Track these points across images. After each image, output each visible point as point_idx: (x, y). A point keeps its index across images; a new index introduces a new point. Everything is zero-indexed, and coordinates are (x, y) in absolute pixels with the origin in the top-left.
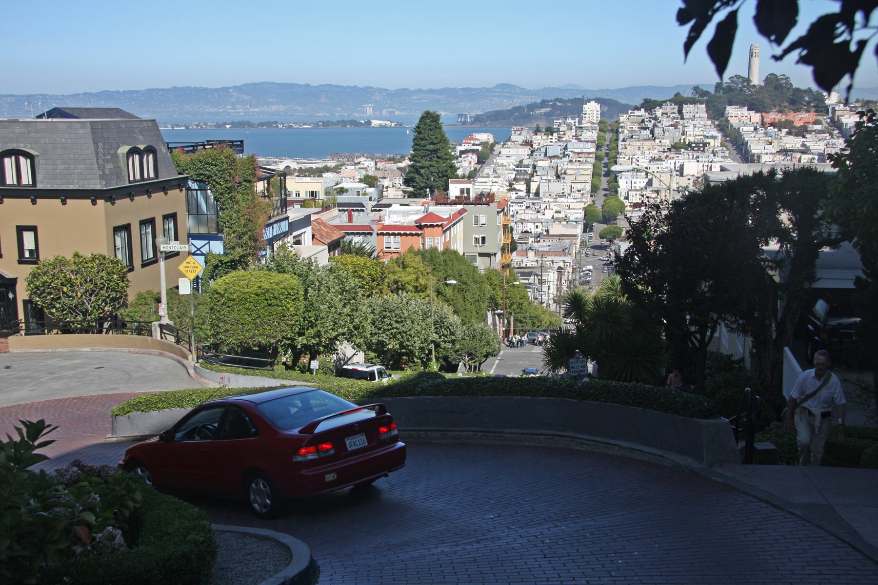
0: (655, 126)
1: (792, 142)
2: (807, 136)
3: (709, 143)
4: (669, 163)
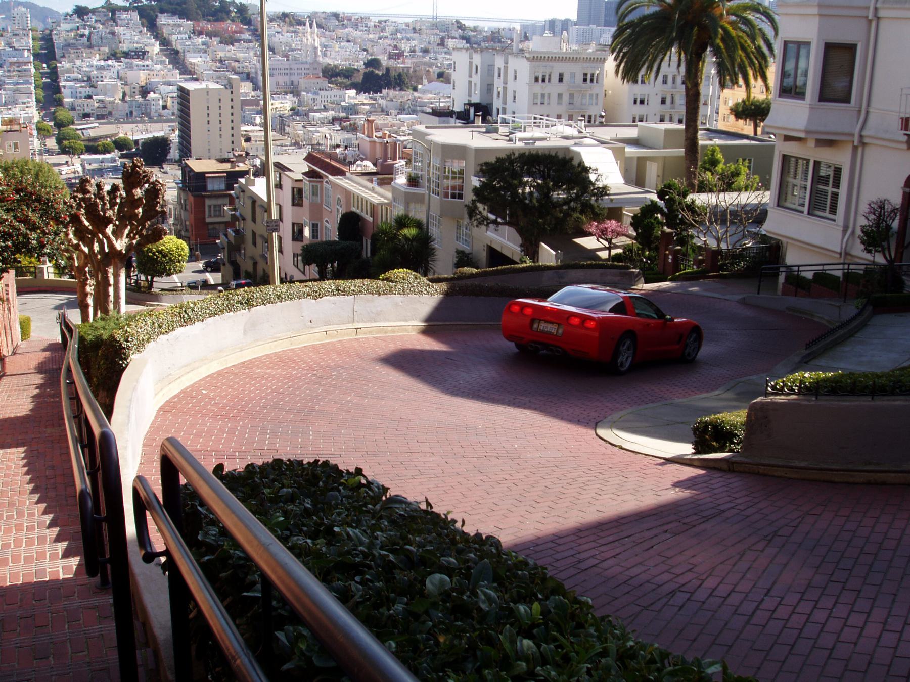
0: (90, 33)
1: (224, 52)
2: (235, 44)
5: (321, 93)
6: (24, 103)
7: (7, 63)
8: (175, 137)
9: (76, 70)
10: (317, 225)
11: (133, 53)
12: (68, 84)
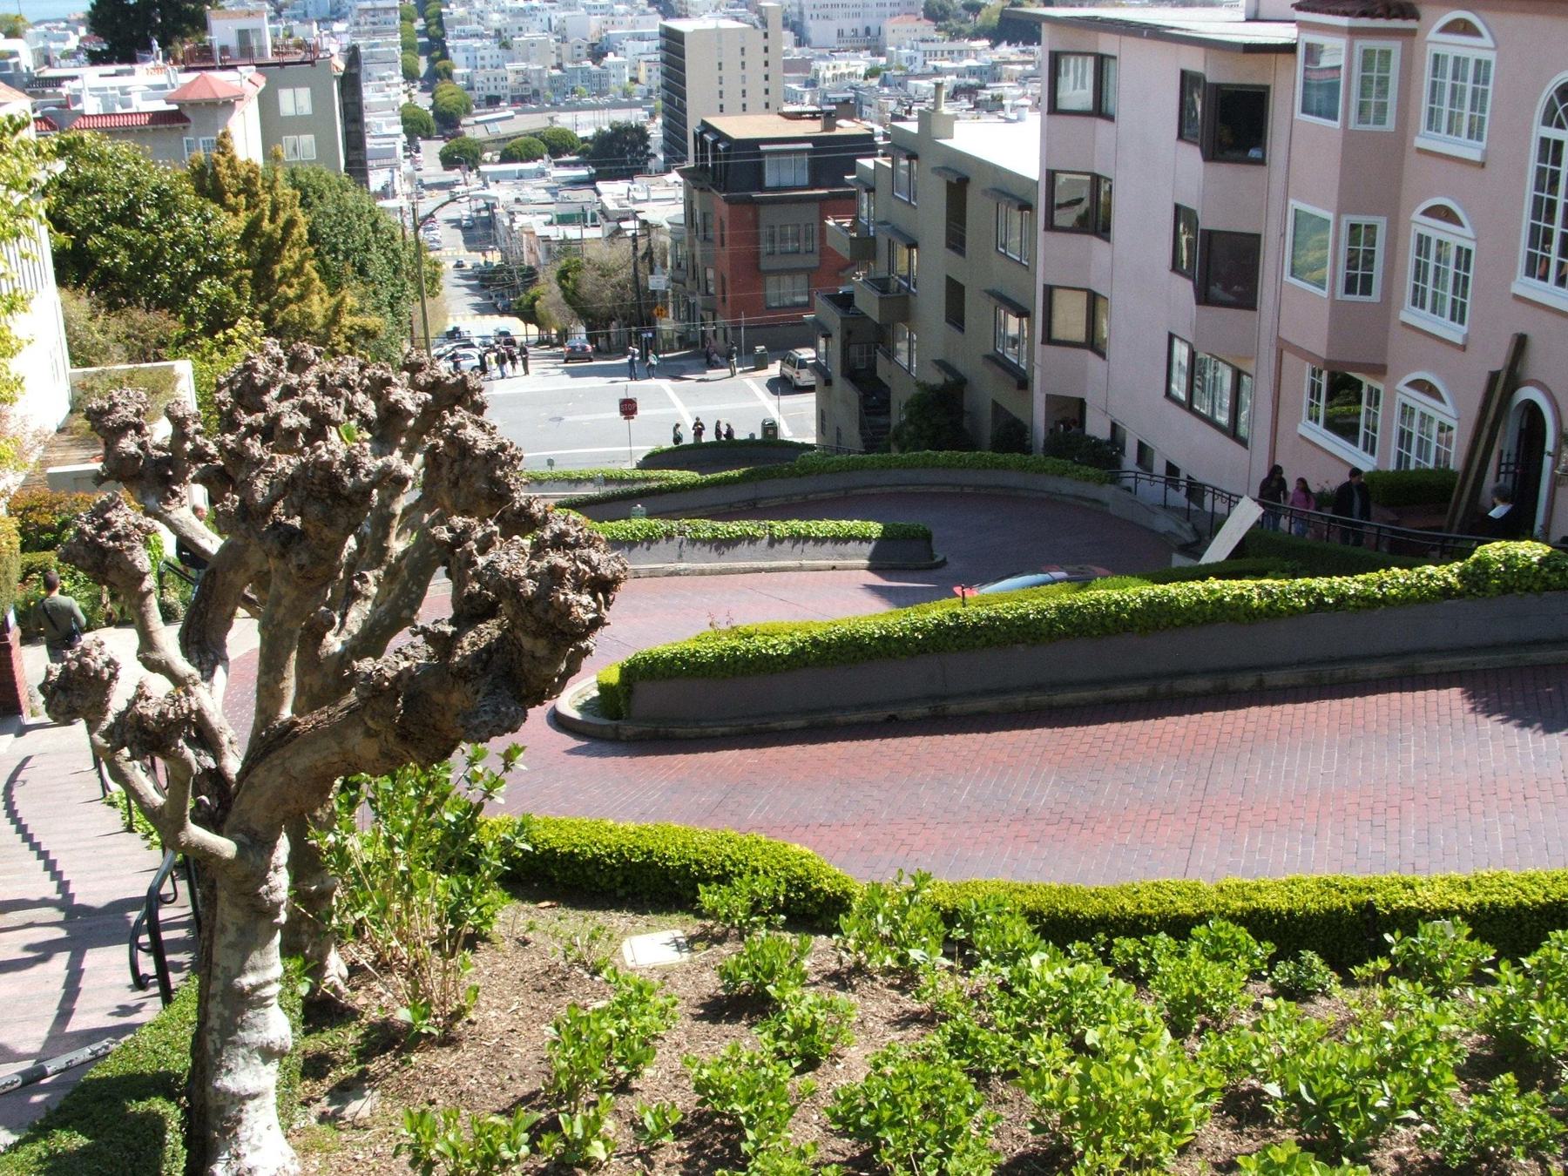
6: (382, 79)
7: (355, 12)
8: (656, 131)
9: (474, 17)
10: (1371, 228)
12: (461, 43)
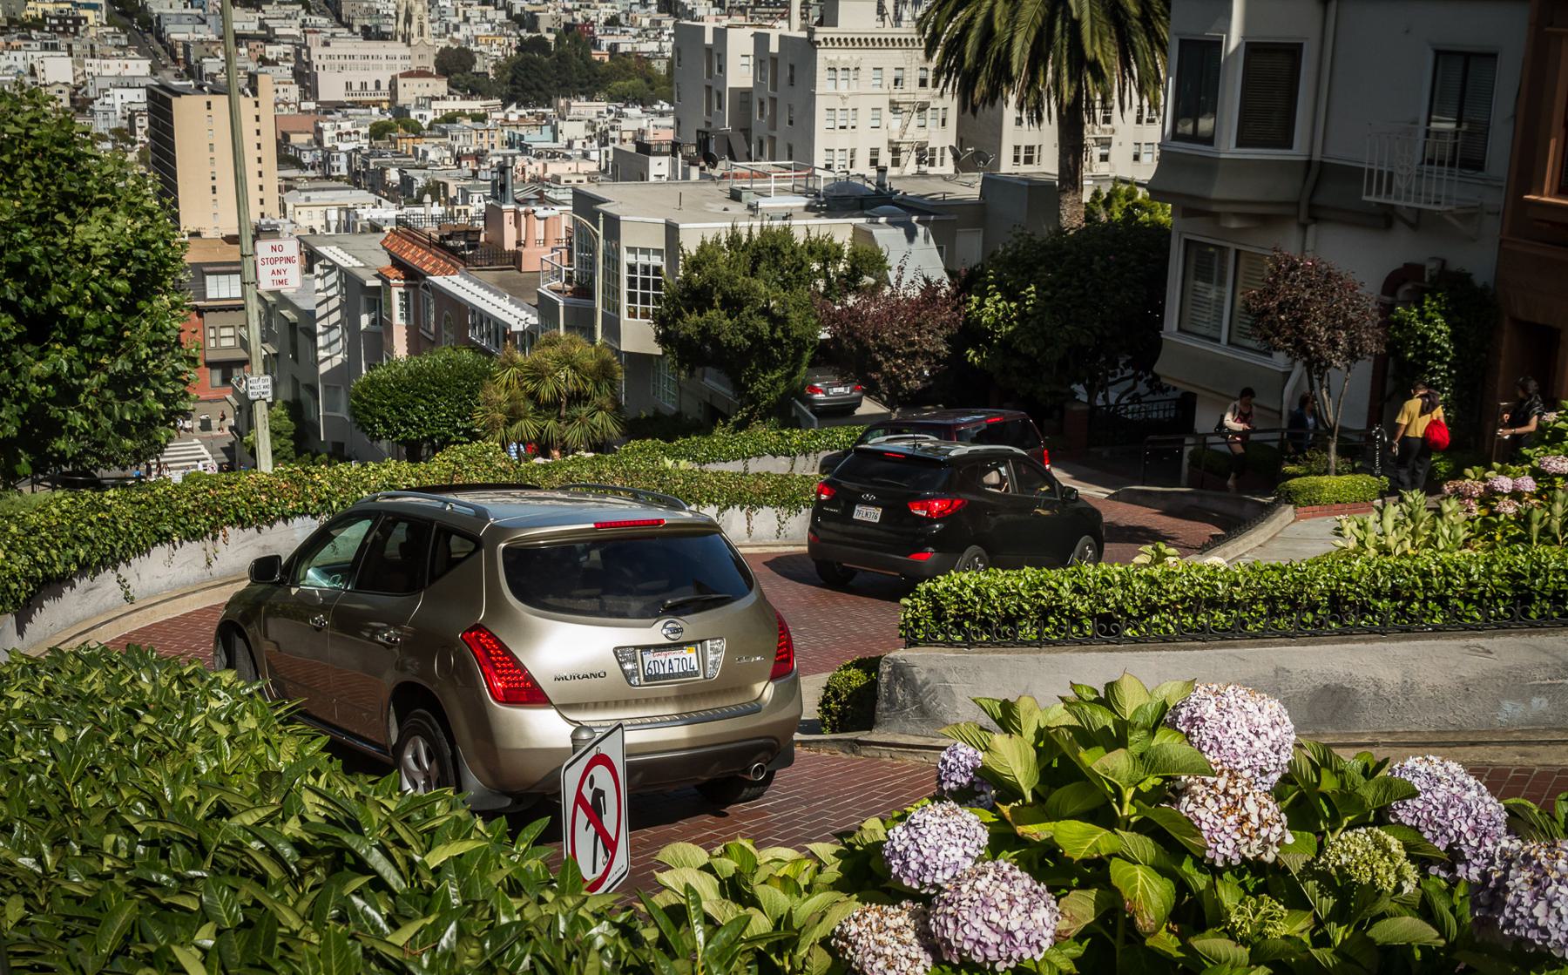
3: (86, 19)
4: (12, 58)
5: (435, 104)
11: (55, 22)
